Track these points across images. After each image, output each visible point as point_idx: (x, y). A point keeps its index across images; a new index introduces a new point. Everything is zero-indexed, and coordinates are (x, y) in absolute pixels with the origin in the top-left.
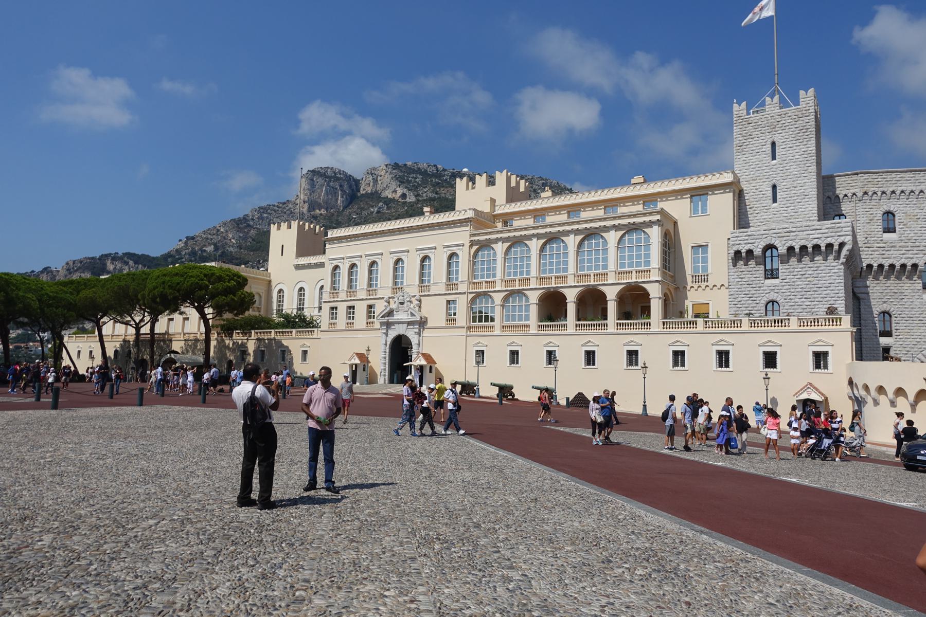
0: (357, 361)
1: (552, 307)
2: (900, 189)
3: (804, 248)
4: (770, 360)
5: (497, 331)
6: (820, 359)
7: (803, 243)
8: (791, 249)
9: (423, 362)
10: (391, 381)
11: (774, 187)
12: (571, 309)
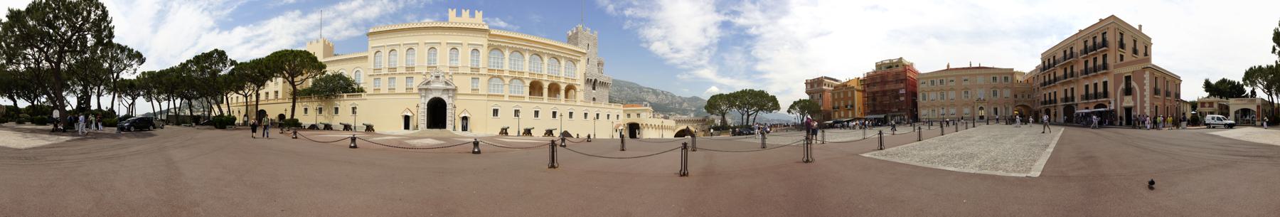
5: (506, 98)
10: (429, 127)
12: (545, 91)
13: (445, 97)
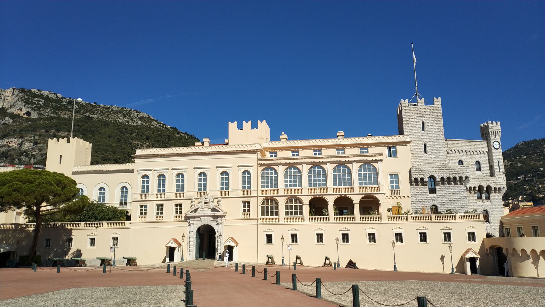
0: (174, 245)
1: (318, 207)
2: (465, 149)
3: (449, 178)
4: (447, 237)
6: (472, 236)
7: (448, 175)
8: (442, 178)
9: (232, 244)
11: (425, 145)
13: (213, 224)
